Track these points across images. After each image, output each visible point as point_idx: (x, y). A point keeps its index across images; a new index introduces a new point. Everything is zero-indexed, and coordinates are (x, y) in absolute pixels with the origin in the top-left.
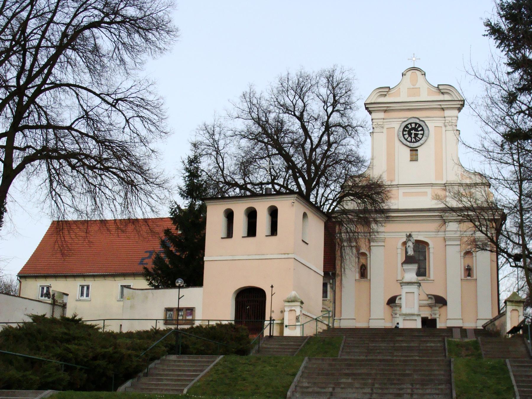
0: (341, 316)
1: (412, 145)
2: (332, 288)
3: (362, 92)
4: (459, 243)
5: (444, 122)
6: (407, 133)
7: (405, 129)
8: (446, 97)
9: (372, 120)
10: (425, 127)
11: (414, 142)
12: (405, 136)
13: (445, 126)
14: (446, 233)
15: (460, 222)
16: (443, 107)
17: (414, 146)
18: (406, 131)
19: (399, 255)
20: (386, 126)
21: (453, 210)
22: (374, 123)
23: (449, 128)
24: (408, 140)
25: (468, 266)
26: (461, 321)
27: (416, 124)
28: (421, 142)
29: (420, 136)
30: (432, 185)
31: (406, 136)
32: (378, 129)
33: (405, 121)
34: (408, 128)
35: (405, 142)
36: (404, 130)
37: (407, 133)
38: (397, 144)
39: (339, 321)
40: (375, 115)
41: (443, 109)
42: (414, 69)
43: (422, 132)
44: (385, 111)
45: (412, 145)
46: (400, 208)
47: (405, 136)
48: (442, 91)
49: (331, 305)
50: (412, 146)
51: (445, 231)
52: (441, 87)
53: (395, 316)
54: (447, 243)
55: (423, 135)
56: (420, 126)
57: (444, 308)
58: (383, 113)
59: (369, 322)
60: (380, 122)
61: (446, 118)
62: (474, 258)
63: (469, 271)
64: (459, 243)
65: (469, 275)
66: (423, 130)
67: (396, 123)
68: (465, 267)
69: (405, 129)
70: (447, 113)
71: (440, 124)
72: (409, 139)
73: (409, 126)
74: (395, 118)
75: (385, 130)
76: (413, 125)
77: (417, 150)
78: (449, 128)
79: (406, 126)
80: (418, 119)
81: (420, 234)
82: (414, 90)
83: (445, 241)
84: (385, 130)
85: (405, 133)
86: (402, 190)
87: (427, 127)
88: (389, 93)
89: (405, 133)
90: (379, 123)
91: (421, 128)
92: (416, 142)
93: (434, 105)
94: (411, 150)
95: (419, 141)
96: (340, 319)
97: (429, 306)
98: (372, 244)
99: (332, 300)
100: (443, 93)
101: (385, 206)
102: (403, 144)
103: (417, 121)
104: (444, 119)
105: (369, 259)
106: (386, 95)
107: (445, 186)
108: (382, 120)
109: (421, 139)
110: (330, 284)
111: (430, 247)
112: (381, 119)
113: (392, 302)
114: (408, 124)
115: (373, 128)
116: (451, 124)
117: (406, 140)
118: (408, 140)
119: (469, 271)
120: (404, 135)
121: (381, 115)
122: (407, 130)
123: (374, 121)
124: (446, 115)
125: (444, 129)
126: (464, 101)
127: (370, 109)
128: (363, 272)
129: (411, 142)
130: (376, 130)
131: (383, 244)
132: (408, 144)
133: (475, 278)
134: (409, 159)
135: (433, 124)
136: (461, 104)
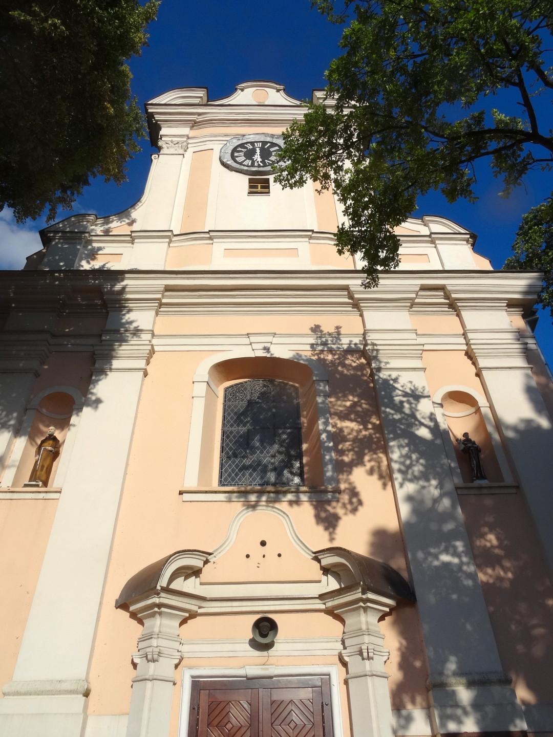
6: (242, 154)
19: (199, 406)
27: (264, 143)
31: (241, 159)
35: (238, 166)
37: (242, 154)
44: (194, 125)
53: (152, 669)
81: (275, 340)
84: (189, 154)
85: (236, 154)
94: (251, 181)
97: (330, 612)
103: (268, 139)
117: (241, 164)
133: (508, 480)
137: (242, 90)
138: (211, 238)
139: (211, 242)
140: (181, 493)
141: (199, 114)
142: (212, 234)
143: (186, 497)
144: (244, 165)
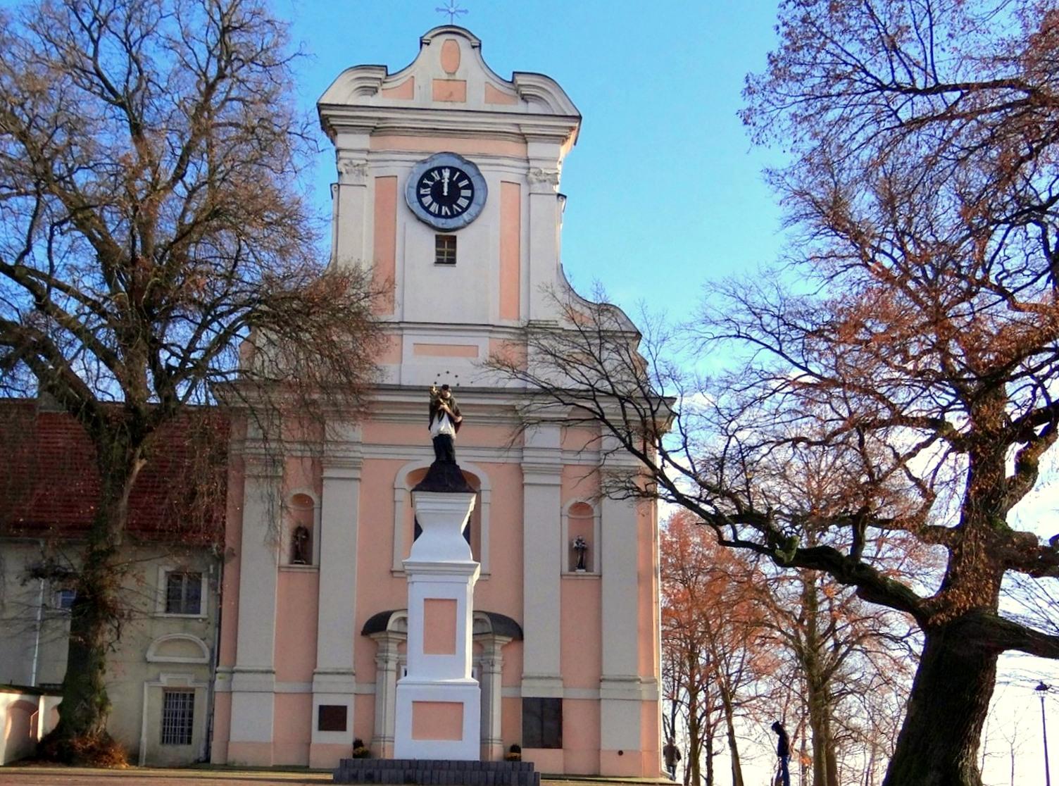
0: (235, 665)
1: (440, 223)
2: (213, 587)
3: (315, 78)
4: (557, 480)
5: (525, 172)
7: (426, 181)
8: (533, 108)
9: (338, 151)
10: (475, 180)
11: (446, 217)
12: (424, 200)
13: (529, 183)
14: (526, 453)
15: (565, 423)
16: (524, 130)
17: (445, 226)
18: (426, 186)
20: (372, 172)
21: (548, 391)
22: (342, 162)
23: (537, 187)
24: (432, 209)
25: (579, 541)
26: (560, 684)
27: (453, 170)
28: (465, 216)
29: (463, 202)
30: (490, 328)
31: (427, 200)
32: (354, 176)
33: (424, 162)
34: (432, 179)
35: (423, 214)
36: (421, 185)
38: (402, 217)
39: (228, 676)
40: (343, 140)
41: (524, 138)
42: (451, 30)
43: (467, 193)
44: (374, 131)
45: (440, 223)
46: (405, 383)
47: (424, 200)
48: (525, 91)
49: (211, 631)
50: (440, 226)
51: (522, 449)
52: (520, 80)
54: (527, 479)
55: (471, 199)
56: (464, 176)
57: (514, 649)
58: (367, 137)
59: (311, 681)
60: (359, 158)
61: (532, 164)
62: (596, 521)
63: (581, 556)
64: (557, 480)
65: (582, 565)
66: (470, 187)
67: (402, 164)
68: (571, 545)
69: (426, 181)
70: (535, 149)
71: (514, 174)
72: (434, 208)
73: (435, 175)
74: (399, 153)
75: (370, 181)
76: (446, 174)
77: (455, 237)
78: (537, 187)
79: (427, 175)
80: (459, 157)
82: (452, 82)
83: (523, 475)
85: (422, 191)
86: (410, 339)
87: (483, 180)
88: (385, 86)
89: (422, 191)
90: (356, 162)
91: (465, 182)
92: (453, 216)
93: (505, 124)
94: (437, 237)
95: (459, 214)
96: (233, 672)
98: (327, 473)
99: (213, 620)
100: (524, 98)
101: (365, 377)
102: (419, 219)
103: (456, 163)
104: (525, 165)
105: (316, 512)
106: (375, 90)
107: (526, 334)
108: (364, 156)
109: (464, 210)
110: (209, 576)
111: (482, 487)
112: (361, 151)
113: (376, 625)
114: (433, 170)
115: (340, 173)
116: (542, 178)
117: (427, 209)
118: (432, 209)
119: (581, 556)
120: (420, 197)
121: (363, 141)
122: (431, 183)
123: (342, 154)
124: (530, 155)
125: (524, 190)
126: (579, 118)
127: (333, 121)
128: (303, 548)
129: (439, 215)
130: (346, 179)
131: (357, 474)
132: (432, 220)
133: (596, 571)
134: (434, 259)
135: (497, 176)
136: (572, 129)
137: (428, 44)
138: (401, 329)
139: (400, 332)
140: (392, 572)
141: (380, 119)
142: (402, 325)
143: (395, 575)
144: (431, 213)
